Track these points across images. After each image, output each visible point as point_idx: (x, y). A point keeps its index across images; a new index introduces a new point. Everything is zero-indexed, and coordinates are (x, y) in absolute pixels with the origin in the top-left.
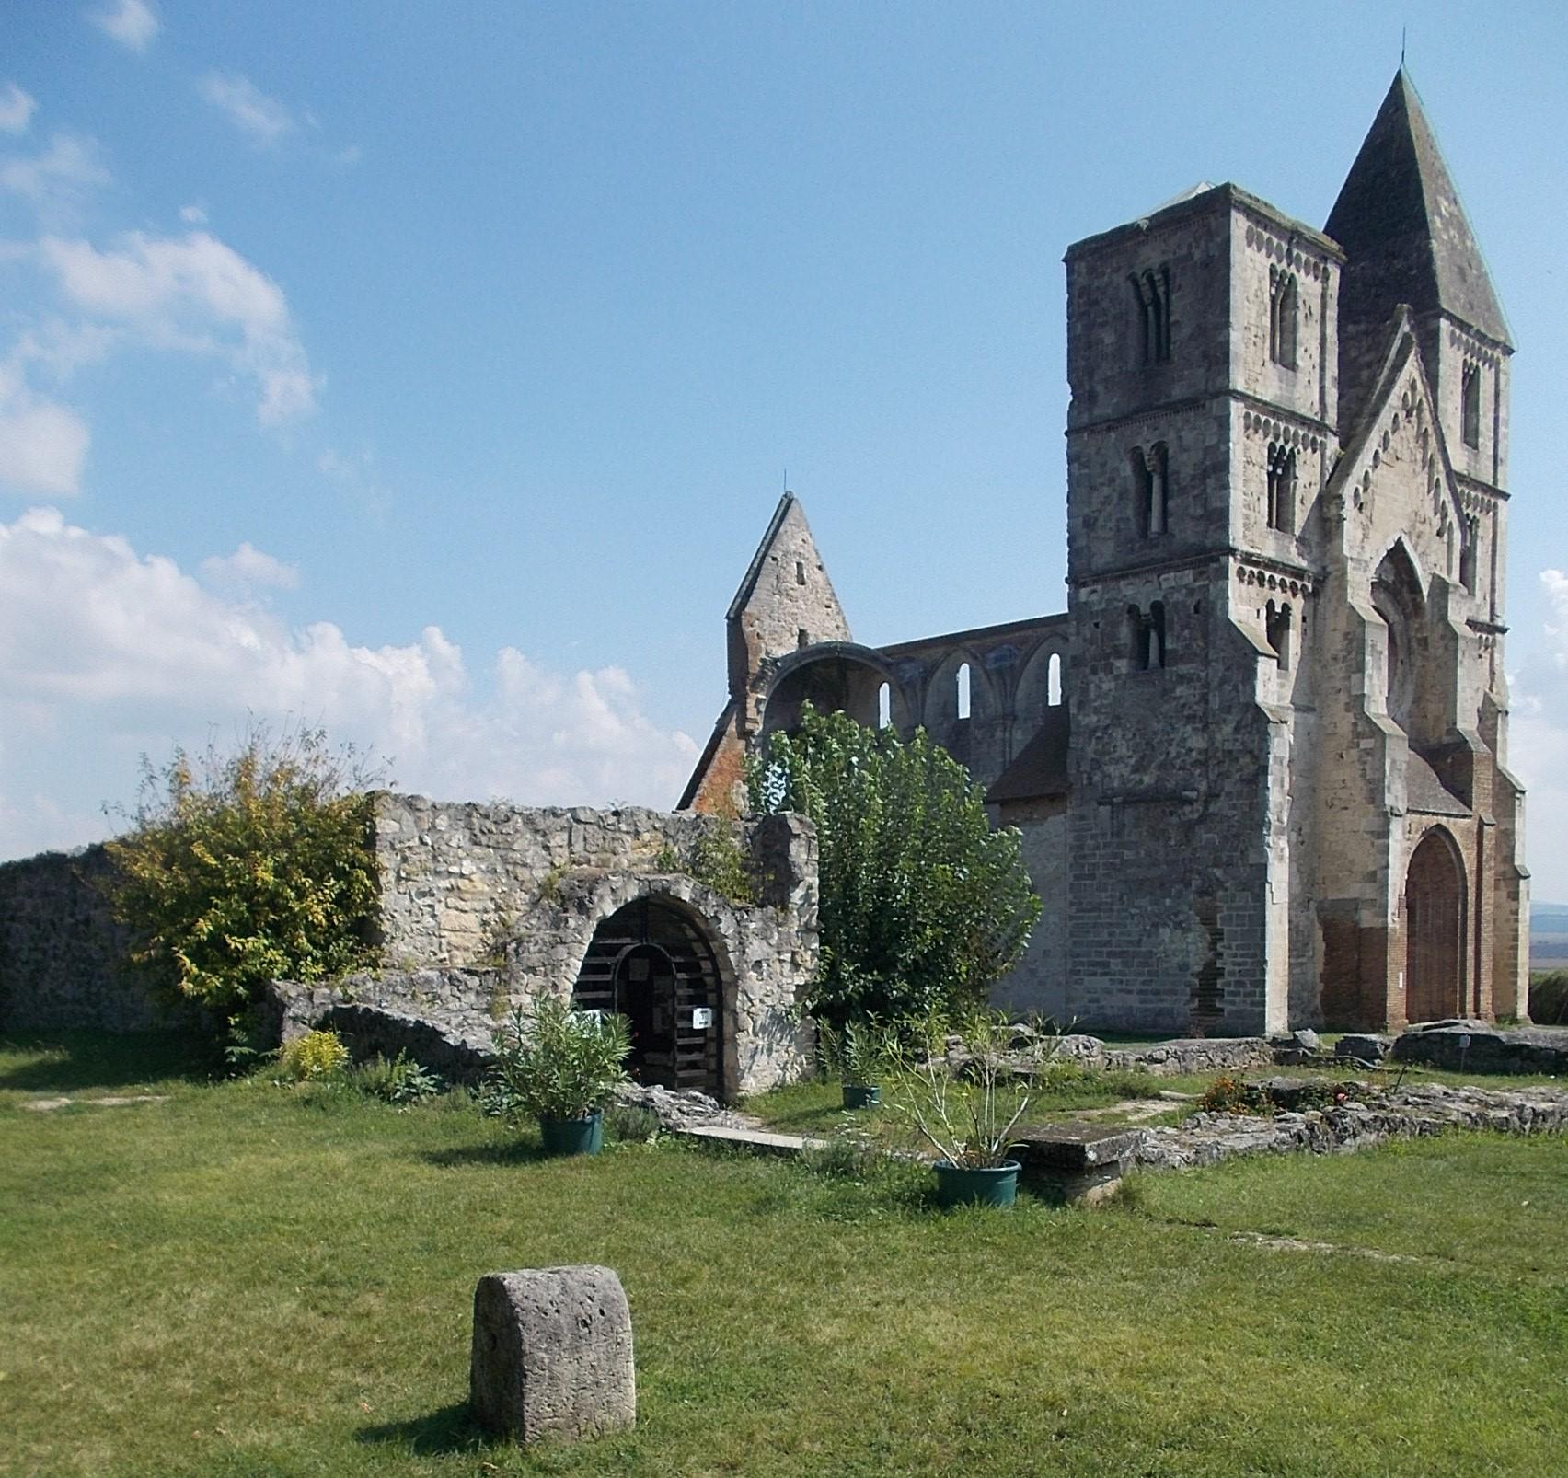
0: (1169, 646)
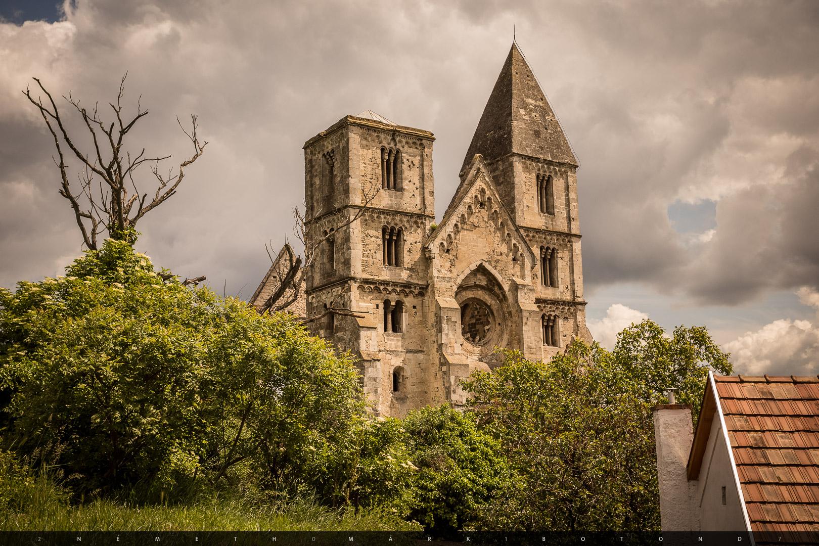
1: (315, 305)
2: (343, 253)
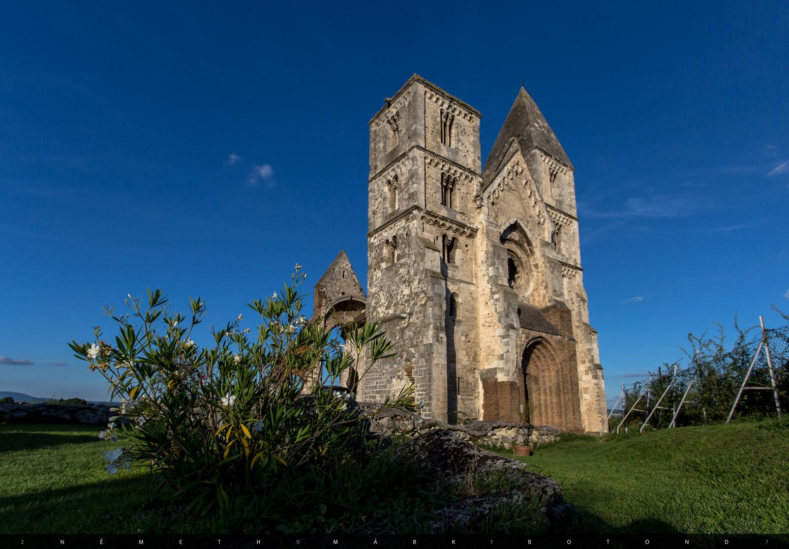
1: (377, 244)
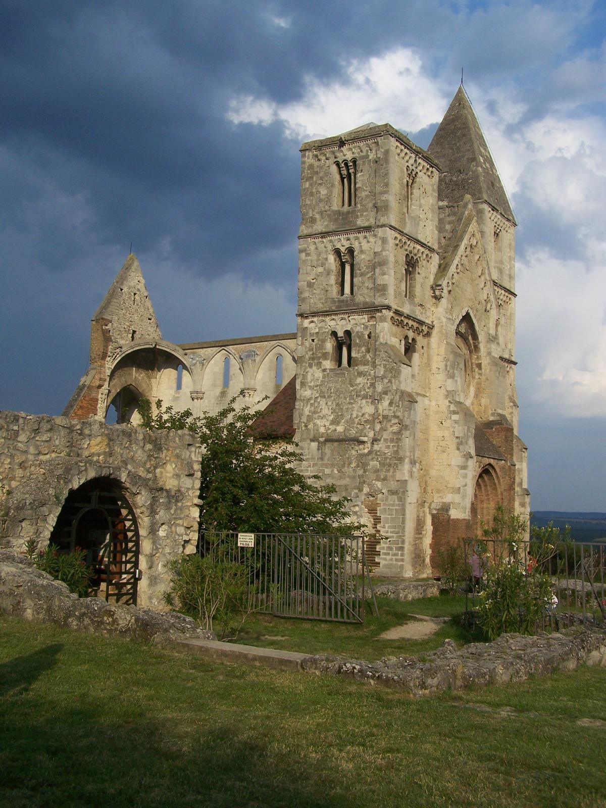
0: (353, 354)
2: (374, 280)
